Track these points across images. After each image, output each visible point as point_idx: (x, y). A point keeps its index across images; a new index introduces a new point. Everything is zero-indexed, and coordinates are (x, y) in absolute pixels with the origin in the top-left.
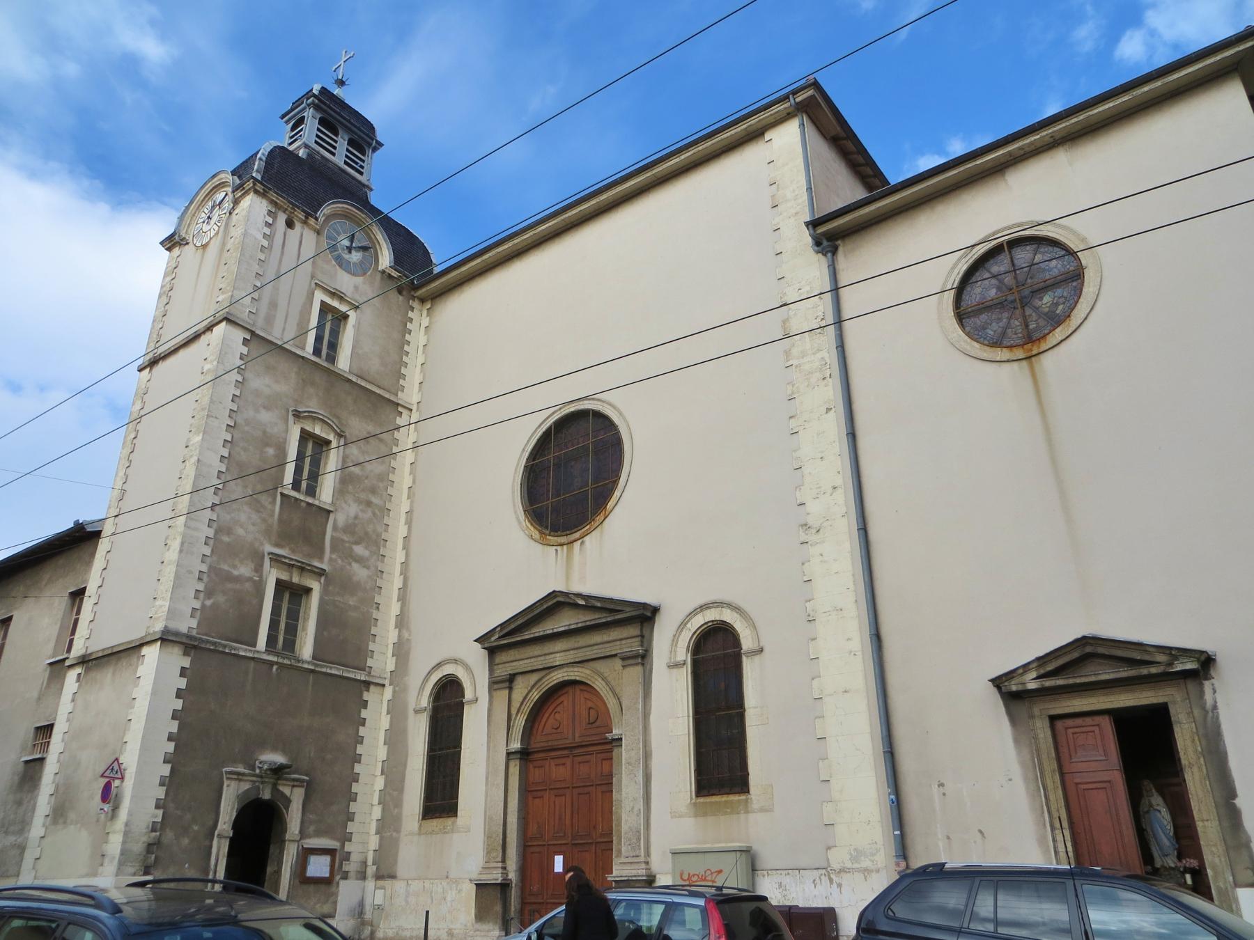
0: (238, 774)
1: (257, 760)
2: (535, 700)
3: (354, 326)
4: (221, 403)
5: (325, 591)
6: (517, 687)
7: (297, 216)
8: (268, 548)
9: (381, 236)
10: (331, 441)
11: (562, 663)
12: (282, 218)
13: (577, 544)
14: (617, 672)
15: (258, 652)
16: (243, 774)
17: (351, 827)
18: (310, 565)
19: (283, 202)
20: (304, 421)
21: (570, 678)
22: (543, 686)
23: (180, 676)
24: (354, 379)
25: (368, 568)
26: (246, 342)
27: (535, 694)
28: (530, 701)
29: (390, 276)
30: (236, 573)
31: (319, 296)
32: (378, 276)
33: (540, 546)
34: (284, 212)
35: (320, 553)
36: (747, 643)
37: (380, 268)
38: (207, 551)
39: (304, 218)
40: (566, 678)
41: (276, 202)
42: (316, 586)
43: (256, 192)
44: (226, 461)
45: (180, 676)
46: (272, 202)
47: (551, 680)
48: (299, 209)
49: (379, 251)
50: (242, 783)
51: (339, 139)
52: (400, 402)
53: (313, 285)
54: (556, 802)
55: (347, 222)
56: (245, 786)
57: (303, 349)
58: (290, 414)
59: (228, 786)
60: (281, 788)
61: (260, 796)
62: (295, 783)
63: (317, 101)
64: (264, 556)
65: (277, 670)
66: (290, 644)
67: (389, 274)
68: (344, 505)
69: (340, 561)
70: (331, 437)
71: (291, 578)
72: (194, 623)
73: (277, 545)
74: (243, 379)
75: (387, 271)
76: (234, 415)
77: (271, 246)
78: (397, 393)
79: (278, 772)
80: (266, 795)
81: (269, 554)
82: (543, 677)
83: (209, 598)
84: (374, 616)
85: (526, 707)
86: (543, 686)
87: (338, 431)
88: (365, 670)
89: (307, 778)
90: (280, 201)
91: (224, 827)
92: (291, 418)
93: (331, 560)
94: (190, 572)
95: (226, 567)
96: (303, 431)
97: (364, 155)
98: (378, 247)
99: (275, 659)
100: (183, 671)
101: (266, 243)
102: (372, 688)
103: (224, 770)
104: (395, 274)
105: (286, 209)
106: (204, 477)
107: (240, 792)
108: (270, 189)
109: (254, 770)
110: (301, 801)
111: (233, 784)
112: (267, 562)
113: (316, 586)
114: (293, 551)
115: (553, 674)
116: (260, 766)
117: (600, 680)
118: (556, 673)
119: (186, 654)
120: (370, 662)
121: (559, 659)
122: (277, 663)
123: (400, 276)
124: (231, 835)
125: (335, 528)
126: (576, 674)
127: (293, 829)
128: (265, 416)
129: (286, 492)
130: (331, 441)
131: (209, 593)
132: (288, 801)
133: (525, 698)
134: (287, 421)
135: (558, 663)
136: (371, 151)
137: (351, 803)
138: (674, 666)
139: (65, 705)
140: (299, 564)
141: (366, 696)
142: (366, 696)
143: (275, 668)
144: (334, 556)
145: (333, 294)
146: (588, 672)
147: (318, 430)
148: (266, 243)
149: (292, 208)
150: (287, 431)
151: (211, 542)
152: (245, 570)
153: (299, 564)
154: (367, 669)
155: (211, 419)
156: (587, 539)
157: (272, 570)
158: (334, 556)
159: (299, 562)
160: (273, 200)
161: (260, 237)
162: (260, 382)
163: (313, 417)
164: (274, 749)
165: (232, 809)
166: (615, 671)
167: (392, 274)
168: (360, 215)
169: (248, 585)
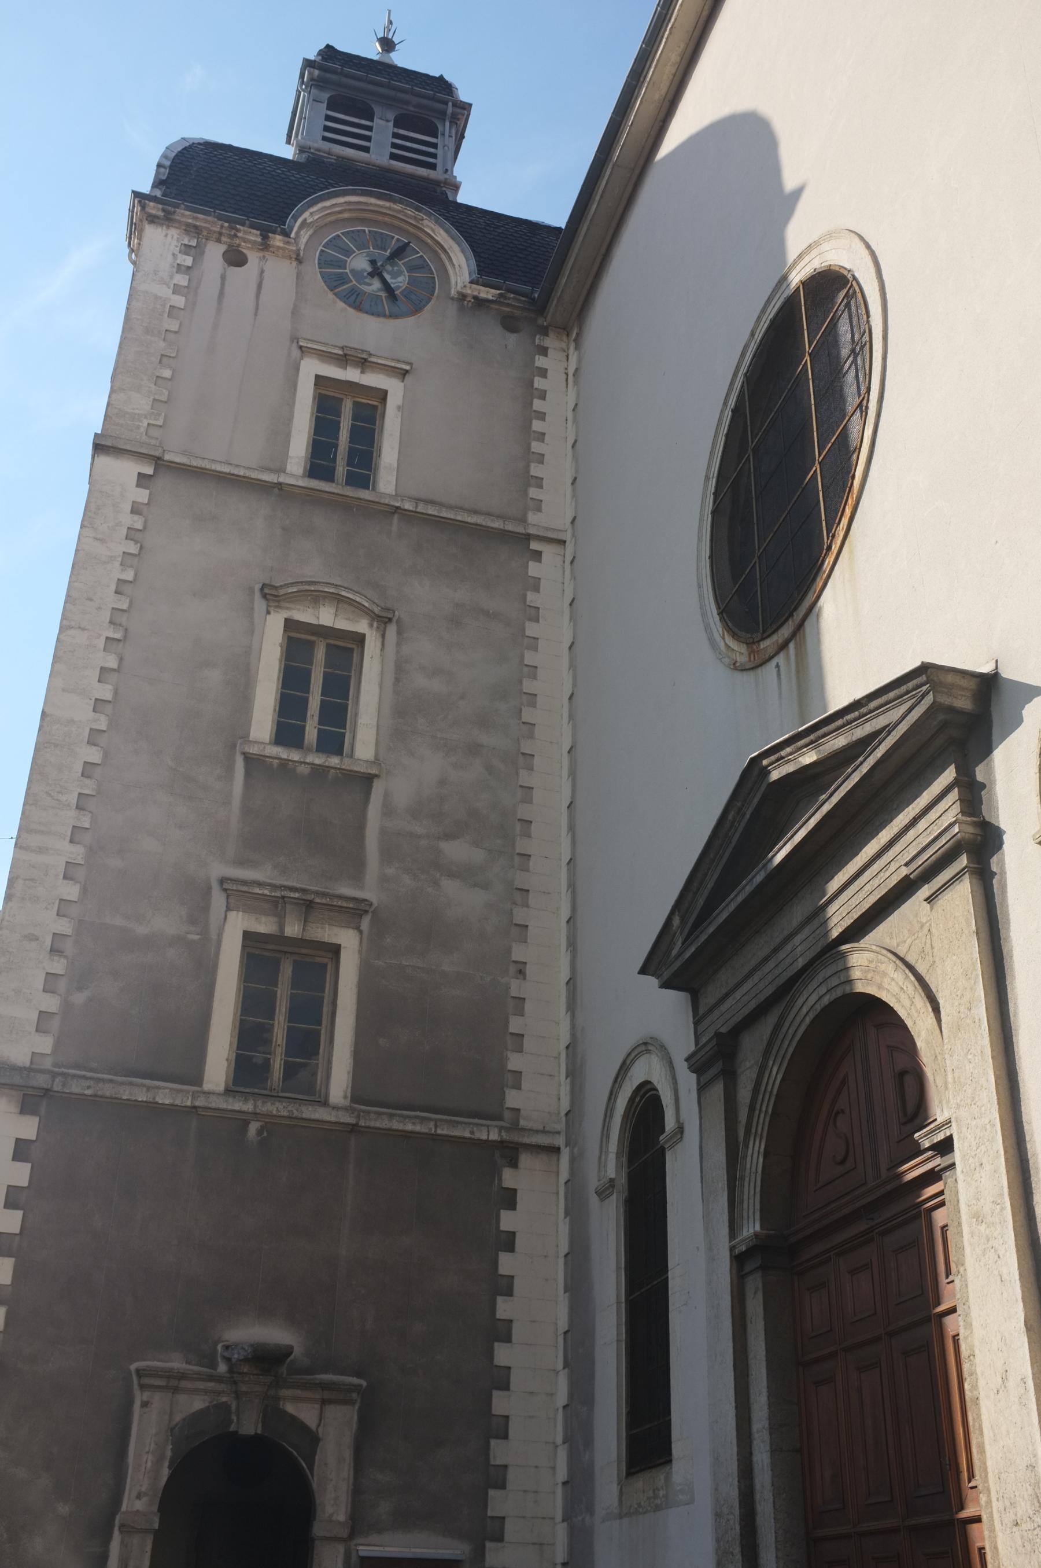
0: (169, 1375)
1: (216, 1343)
4: (91, 600)
7: (245, 241)
9: (442, 232)
10: (364, 635)
12: (215, 252)
15: (208, 1093)
16: (182, 1376)
17: (498, 1503)
18: (324, 895)
19: (206, 221)
20: (287, 605)
23: (14, 1159)
25: (485, 886)
26: (142, 480)
29: (480, 303)
30: (141, 930)
31: (311, 368)
32: (452, 309)
34: (219, 241)
35: (356, 867)
37: (453, 292)
38: (71, 891)
39: (259, 239)
41: (196, 227)
42: (348, 940)
43: (152, 219)
44: (109, 709)
45: (14, 1159)
46: (194, 230)
47: (798, 1019)
48: (243, 225)
49: (446, 262)
50: (182, 1398)
51: (377, 123)
52: (532, 531)
53: (296, 353)
55: (366, 229)
58: (257, 595)
59: (145, 1404)
60: (290, 1408)
61: (232, 1428)
62: (327, 1395)
63: (316, 72)
64: (209, 889)
65: (260, 1132)
67: (476, 298)
69: (407, 880)
70: (362, 626)
71: (282, 926)
72: (45, 1044)
73: (241, 862)
74: (141, 548)
75: (469, 291)
76: (123, 619)
78: (525, 515)
80: (249, 1425)
81: (222, 881)
82: (782, 1018)
83: (80, 989)
84: (514, 993)
85: (762, 1115)
86: (786, 1043)
87: (376, 610)
88: (500, 1118)
89: (364, 1383)
90: (202, 220)
91: (139, 1505)
92: (260, 604)
95: (119, 921)
96: (290, 625)
98: (443, 257)
99: (248, 1107)
100: (21, 1150)
101: (179, 301)
102: (526, 1160)
103: (133, 1367)
104: (488, 293)
105: (220, 234)
106: (56, 745)
107: (178, 1418)
108: (177, 206)
109: (213, 1365)
110: (348, 1439)
111: (158, 1400)
112: (218, 900)
113: (348, 940)
116: (226, 1354)
119: (26, 1108)
120: (513, 1098)
122: (255, 1115)
123: (500, 295)
124: (156, 1526)
125: (388, 810)
127: (329, 1510)
129: (254, 750)
130: (364, 635)
131: (81, 978)
132: (312, 1440)
135: (800, 963)
136: (447, 124)
137: (493, 1442)
140: (297, 895)
141: (509, 1178)
142: (509, 1178)
143: (253, 1128)
144: (390, 871)
145: (344, 359)
147: (326, 616)
148: (179, 301)
149: (231, 228)
151: (81, 874)
153: (297, 895)
154: (507, 1115)
155: (72, 632)
157: (232, 915)
158: (390, 871)
159: (292, 889)
160: (188, 225)
161: (165, 292)
163: (316, 597)
165: (161, 1458)
167: (483, 295)
168: (390, 208)
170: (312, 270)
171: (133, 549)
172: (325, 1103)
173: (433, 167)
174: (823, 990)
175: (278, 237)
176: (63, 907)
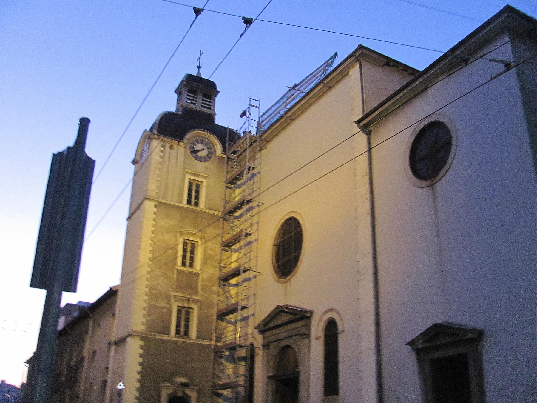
3: (206, 186)
5: (199, 309)
8: (173, 293)
12: (168, 145)
13: (288, 282)
18: (191, 298)
24: (207, 211)
26: (156, 206)
31: (188, 177)
32: (217, 159)
33: (278, 283)
35: (196, 292)
36: (340, 328)
42: (195, 307)
56: (170, 391)
57: (181, 202)
66: (186, 333)
68: (207, 270)
77: (163, 160)
79: (185, 385)
80: (180, 394)
90: (165, 139)
92: (178, 235)
93: (202, 295)
94: (140, 307)
95: (154, 303)
97: (211, 99)
98: (215, 145)
111: (165, 390)
114: (184, 293)
121: (282, 336)
125: (203, 280)
128: (166, 237)
131: (149, 315)
134: (176, 236)
138: (318, 338)
139: (111, 360)
145: (194, 175)
148: (161, 160)
150: (177, 240)
152: (163, 304)
156: (292, 280)
162: (165, 222)
164: (182, 376)
169: (165, 310)
170: (189, 150)
171: (154, 223)
172: (191, 339)
173: (210, 109)
175: (181, 143)
176: (145, 301)
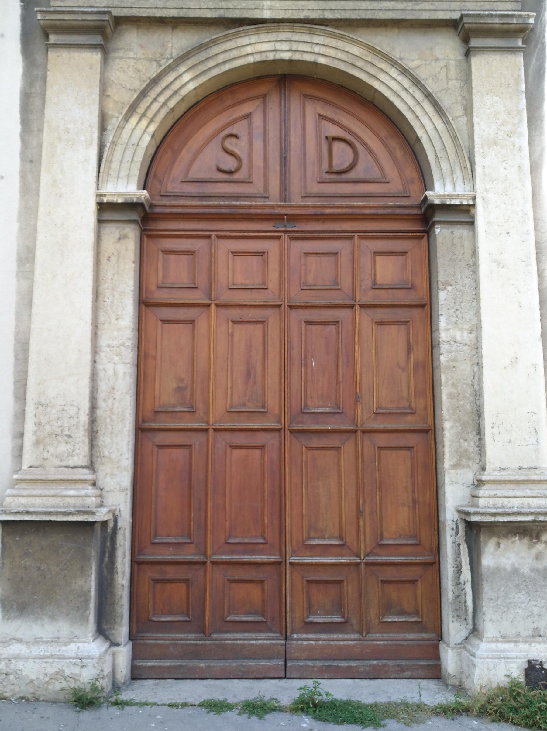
2: (184, 92)
6: (121, 54)
11: (280, 15)
14: (441, 64)
21: (297, 57)
22: (211, 63)
27: (187, 77)
28: (168, 93)
40: (286, 56)
54: (236, 338)
82: (214, 42)
85: (156, 106)
86: (211, 63)
115: (245, 41)
117: (394, 73)
118: (254, 39)
126: (317, 49)
133: (155, 81)
135: (267, 14)
146: (355, 50)
166: (437, 60)
174: (285, 46)
